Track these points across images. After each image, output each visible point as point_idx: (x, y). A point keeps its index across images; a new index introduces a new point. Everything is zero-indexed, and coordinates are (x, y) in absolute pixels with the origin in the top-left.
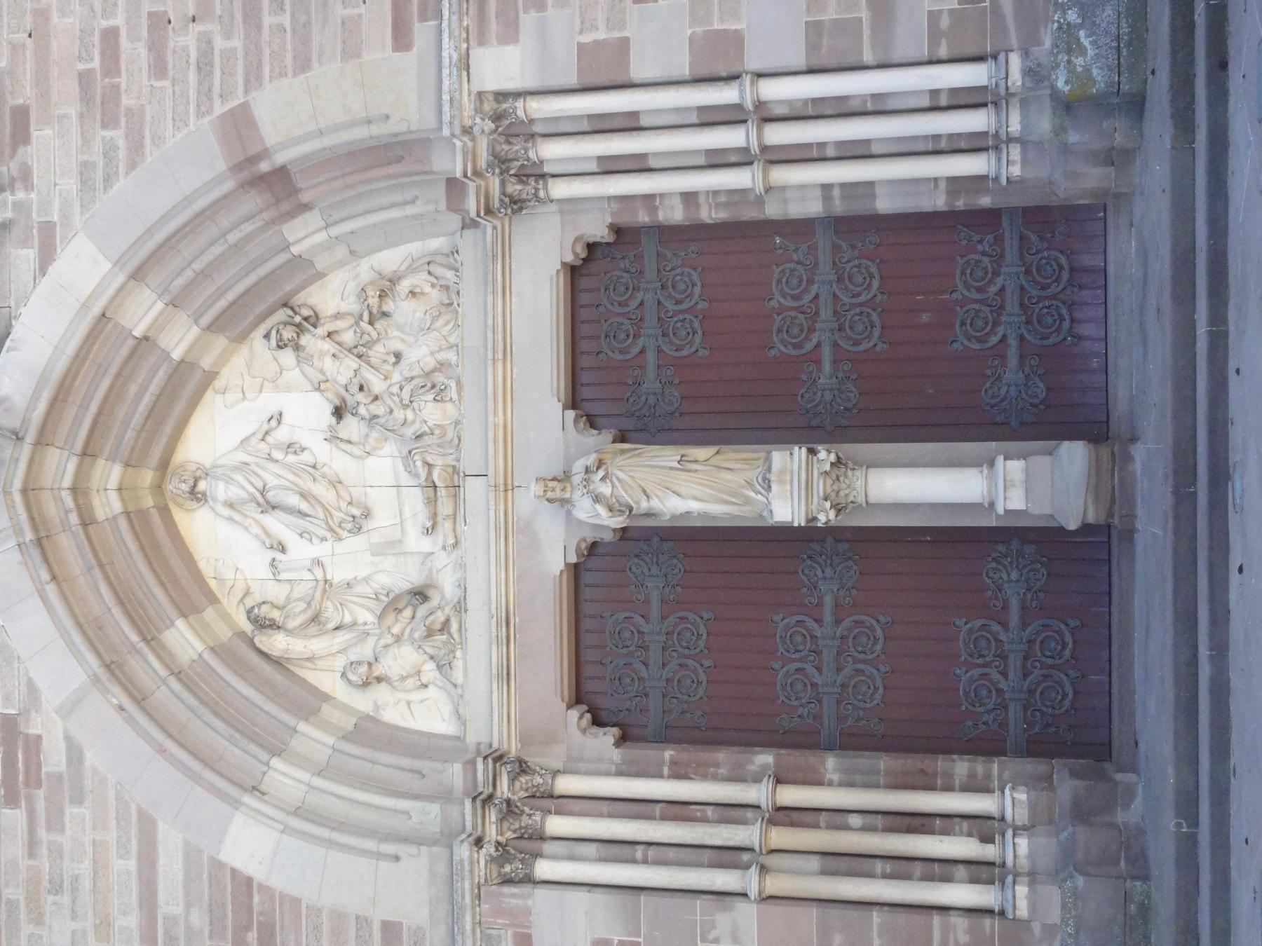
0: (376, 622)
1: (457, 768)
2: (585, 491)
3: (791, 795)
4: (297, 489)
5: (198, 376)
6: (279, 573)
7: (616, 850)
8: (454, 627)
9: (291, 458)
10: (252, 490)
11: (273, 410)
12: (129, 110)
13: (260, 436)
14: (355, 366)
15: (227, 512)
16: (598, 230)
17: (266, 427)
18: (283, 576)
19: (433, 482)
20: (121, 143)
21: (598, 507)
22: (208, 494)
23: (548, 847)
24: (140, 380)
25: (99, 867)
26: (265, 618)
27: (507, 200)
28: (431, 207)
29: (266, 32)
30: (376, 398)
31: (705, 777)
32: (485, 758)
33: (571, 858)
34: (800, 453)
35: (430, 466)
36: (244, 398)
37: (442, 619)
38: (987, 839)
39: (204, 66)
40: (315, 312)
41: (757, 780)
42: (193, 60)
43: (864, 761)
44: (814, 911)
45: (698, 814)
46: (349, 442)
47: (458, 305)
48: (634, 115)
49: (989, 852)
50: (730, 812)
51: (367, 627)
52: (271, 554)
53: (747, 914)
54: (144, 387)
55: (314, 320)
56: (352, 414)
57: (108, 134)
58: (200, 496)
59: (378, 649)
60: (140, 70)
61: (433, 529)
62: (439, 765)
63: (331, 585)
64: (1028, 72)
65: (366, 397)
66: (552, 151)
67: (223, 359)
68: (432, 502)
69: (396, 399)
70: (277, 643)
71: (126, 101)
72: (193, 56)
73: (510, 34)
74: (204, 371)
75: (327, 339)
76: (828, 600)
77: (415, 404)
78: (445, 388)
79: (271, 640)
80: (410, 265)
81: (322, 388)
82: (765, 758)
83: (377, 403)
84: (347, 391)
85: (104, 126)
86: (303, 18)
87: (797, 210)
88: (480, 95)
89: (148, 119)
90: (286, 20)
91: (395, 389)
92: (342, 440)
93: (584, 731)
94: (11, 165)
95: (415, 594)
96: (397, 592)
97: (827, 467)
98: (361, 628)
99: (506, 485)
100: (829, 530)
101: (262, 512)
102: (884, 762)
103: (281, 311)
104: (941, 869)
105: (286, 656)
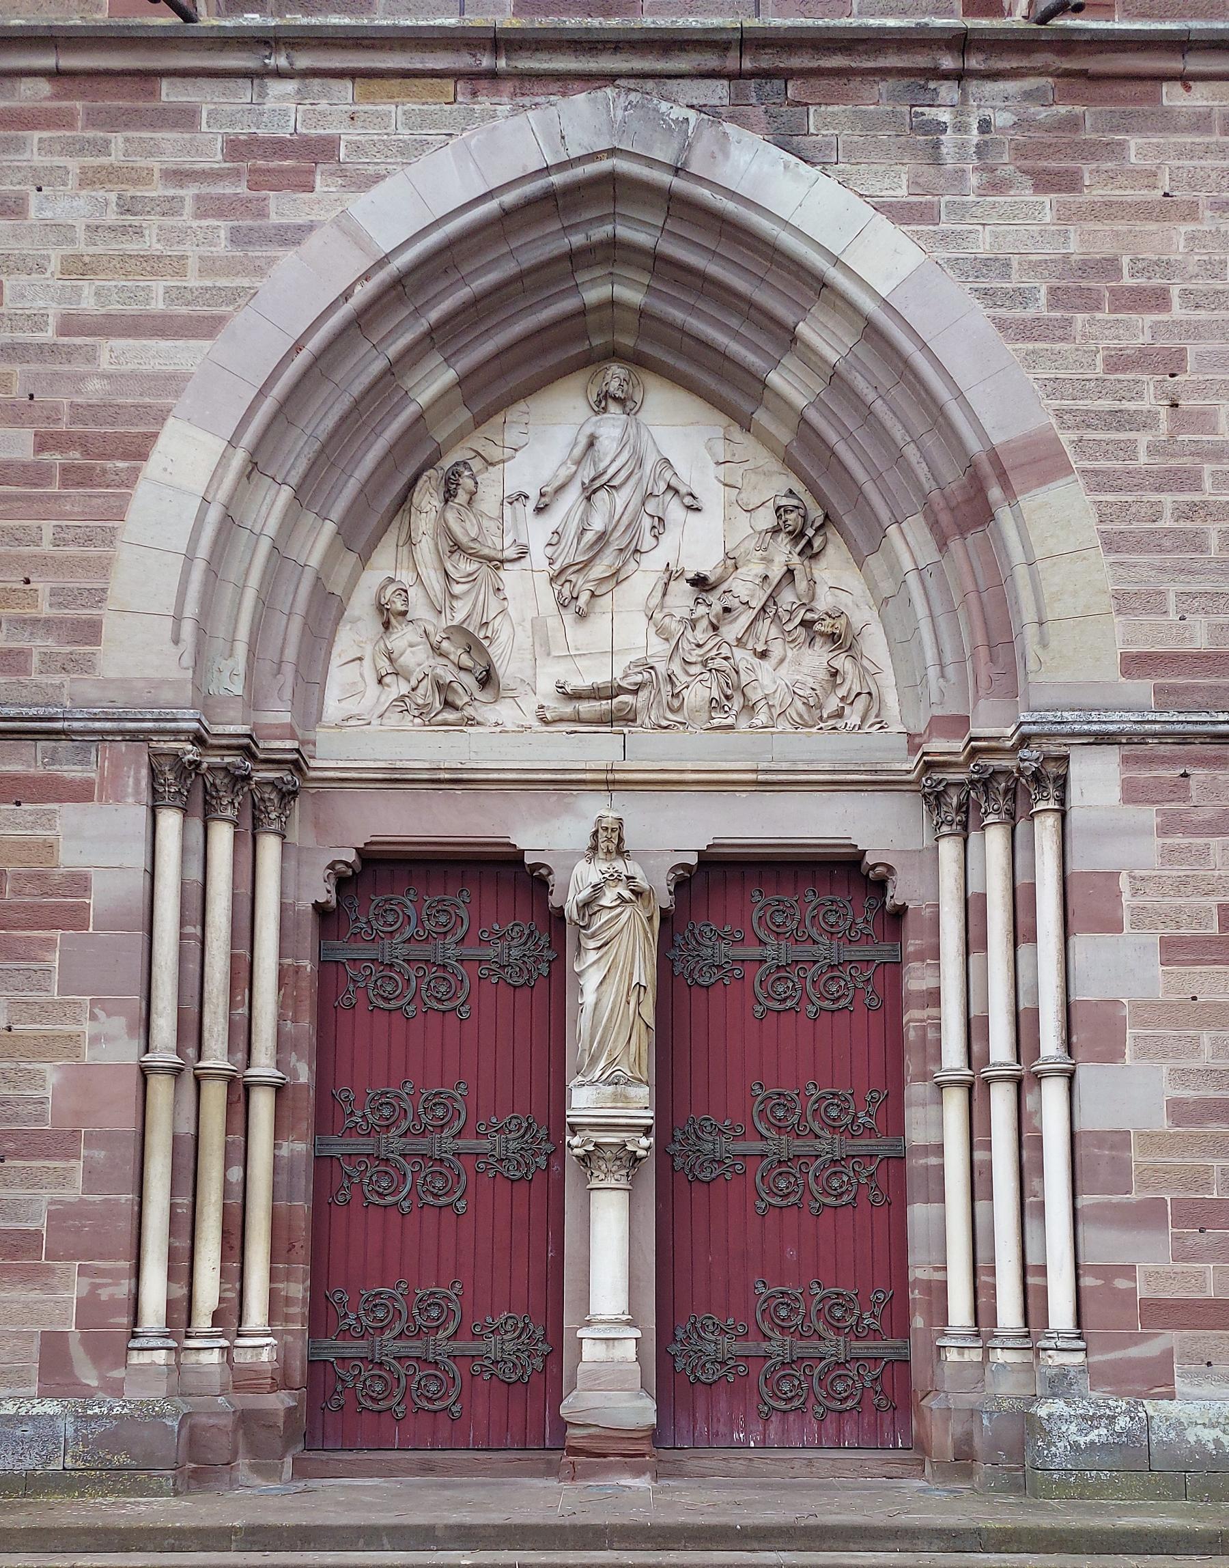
0: (454, 623)
1: (286, 718)
2: (607, 875)
3: (263, 1103)
4: (610, 529)
5: (746, 406)
6: (511, 503)
7: (196, 902)
8: (450, 716)
9: (647, 522)
10: (611, 472)
11: (704, 500)
12: (1070, 322)
13: (674, 482)
14: (752, 604)
15: (583, 441)
16: (899, 893)
17: (683, 490)
18: (508, 509)
19: (618, 695)
20: (1030, 313)
21: (590, 890)
22: (605, 415)
23: (197, 824)
24: (742, 330)
25: (152, 264)
26: (458, 484)
27: (940, 788)
28: (935, 698)
29: (1155, 497)
30: (715, 628)
31: (282, 1005)
32: (298, 751)
33: (184, 850)
34: (647, 1117)
35: (635, 692)
36: (718, 463)
37: (459, 703)
38: (217, 1318)
39: (1118, 420)
40: (818, 554)
41: (278, 1065)
42: (1126, 405)
43: (304, 1184)
44: (130, 1126)
45: (239, 998)
46: (664, 594)
47: (821, 729)
48: (1033, 938)
49: (203, 1322)
51: (448, 610)
52: (534, 494)
54: (736, 335)
55: (810, 553)
56: (697, 599)
57: (1043, 295)
58: (603, 404)
59: (420, 623)
60: (1117, 337)
61: (564, 693)
62: (288, 694)
63: (498, 568)
64: (1063, 1369)
65: (717, 616)
66: (995, 840)
67: (765, 439)
68: (595, 694)
69: (714, 652)
70: (427, 500)
71: (1080, 318)
72: (1131, 406)
73: (1132, 793)
74: (753, 413)
75: (785, 568)
76: (485, 1145)
77: (707, 675)
78: (726, 712)
79: (431, 491)
80: (868, 671)
81: (730, 562)
82: (304, 1074)
83: (710, 628)
84: (725, 592)
85: (1053, 291)
86: (1167, 543)
87: (913, 1115)
88: (1065, 759)
89: (1058, 346)
90: (1167, 523)
91: (725, 651)
92: (666, 584)
93: (331, 866)
94: (1012, 167)
95: (487, 671)
96: (489, 650)
97: (630, 1148)
98: (448, 603)
99: (614, 782)
100: (560, 1150)
101: (583, 484)
102: (302, 1205)
103: (820, 512)
105: (413, 510)
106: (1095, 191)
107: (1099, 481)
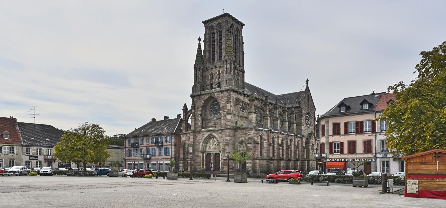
50: (204, 159)
53: (200, 160)
73: (222, 152)
104: (202, 166)
106: (222, 134)
107: (222, 143)
